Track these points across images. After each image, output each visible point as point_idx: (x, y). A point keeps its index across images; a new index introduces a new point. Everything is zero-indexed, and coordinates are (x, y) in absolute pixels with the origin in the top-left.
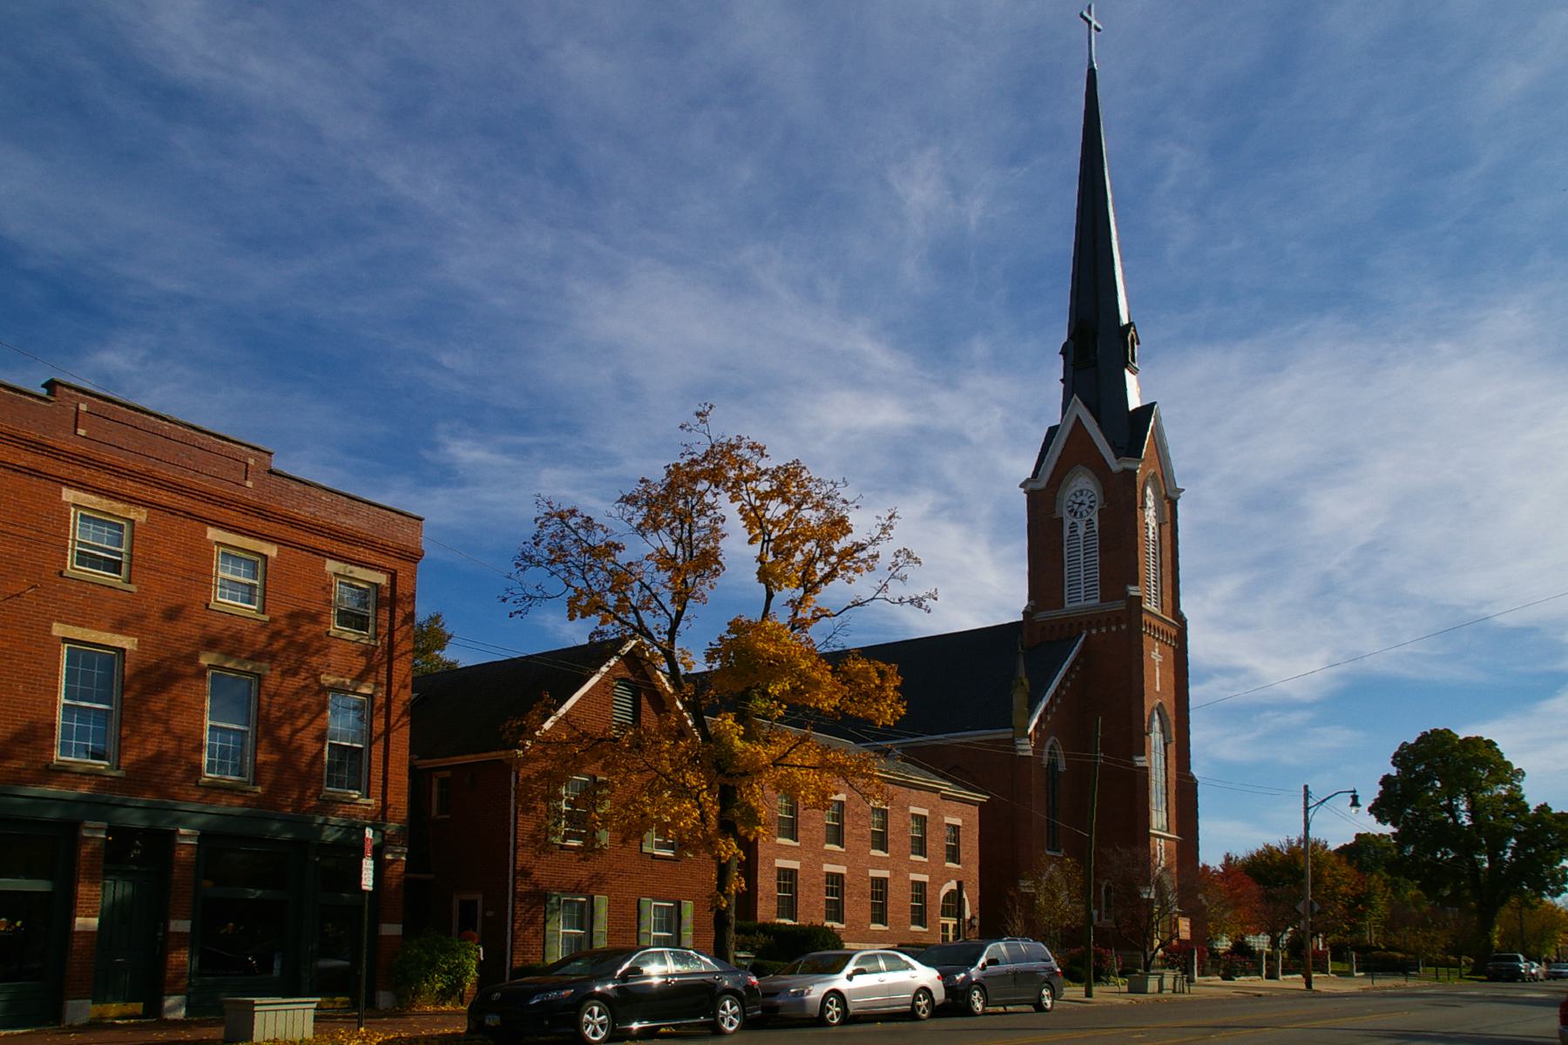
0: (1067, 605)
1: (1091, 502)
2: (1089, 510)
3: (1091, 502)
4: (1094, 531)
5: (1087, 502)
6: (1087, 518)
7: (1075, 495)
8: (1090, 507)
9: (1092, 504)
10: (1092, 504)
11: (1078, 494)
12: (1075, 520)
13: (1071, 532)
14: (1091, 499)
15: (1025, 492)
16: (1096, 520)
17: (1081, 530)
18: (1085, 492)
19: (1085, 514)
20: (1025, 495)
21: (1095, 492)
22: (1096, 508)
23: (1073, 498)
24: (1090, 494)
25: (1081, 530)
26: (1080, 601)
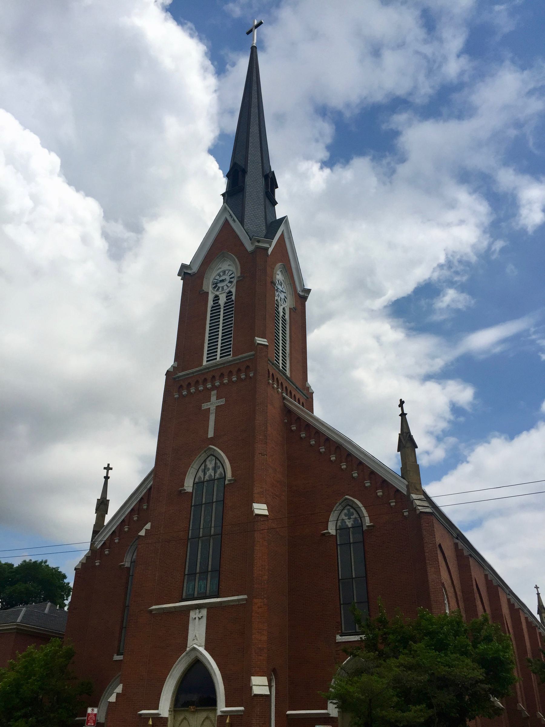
0: (205, 363)
1: (231, 278)
2: (229, 285)
3: (231, 278)
4: (233, 301)
6: (227, 291)
8: (231, 282)
9: (232, 280)
10: (232, 280)
11: (221, 274)
12: (218, 293)
13: (214, 304)
14: (231, 276)
16: (234, 290)
18: (227, 272)
19: (225, 288)
21: (234, 270)
23: (218, 277)
24: (230, 273)
25: (223, 300)
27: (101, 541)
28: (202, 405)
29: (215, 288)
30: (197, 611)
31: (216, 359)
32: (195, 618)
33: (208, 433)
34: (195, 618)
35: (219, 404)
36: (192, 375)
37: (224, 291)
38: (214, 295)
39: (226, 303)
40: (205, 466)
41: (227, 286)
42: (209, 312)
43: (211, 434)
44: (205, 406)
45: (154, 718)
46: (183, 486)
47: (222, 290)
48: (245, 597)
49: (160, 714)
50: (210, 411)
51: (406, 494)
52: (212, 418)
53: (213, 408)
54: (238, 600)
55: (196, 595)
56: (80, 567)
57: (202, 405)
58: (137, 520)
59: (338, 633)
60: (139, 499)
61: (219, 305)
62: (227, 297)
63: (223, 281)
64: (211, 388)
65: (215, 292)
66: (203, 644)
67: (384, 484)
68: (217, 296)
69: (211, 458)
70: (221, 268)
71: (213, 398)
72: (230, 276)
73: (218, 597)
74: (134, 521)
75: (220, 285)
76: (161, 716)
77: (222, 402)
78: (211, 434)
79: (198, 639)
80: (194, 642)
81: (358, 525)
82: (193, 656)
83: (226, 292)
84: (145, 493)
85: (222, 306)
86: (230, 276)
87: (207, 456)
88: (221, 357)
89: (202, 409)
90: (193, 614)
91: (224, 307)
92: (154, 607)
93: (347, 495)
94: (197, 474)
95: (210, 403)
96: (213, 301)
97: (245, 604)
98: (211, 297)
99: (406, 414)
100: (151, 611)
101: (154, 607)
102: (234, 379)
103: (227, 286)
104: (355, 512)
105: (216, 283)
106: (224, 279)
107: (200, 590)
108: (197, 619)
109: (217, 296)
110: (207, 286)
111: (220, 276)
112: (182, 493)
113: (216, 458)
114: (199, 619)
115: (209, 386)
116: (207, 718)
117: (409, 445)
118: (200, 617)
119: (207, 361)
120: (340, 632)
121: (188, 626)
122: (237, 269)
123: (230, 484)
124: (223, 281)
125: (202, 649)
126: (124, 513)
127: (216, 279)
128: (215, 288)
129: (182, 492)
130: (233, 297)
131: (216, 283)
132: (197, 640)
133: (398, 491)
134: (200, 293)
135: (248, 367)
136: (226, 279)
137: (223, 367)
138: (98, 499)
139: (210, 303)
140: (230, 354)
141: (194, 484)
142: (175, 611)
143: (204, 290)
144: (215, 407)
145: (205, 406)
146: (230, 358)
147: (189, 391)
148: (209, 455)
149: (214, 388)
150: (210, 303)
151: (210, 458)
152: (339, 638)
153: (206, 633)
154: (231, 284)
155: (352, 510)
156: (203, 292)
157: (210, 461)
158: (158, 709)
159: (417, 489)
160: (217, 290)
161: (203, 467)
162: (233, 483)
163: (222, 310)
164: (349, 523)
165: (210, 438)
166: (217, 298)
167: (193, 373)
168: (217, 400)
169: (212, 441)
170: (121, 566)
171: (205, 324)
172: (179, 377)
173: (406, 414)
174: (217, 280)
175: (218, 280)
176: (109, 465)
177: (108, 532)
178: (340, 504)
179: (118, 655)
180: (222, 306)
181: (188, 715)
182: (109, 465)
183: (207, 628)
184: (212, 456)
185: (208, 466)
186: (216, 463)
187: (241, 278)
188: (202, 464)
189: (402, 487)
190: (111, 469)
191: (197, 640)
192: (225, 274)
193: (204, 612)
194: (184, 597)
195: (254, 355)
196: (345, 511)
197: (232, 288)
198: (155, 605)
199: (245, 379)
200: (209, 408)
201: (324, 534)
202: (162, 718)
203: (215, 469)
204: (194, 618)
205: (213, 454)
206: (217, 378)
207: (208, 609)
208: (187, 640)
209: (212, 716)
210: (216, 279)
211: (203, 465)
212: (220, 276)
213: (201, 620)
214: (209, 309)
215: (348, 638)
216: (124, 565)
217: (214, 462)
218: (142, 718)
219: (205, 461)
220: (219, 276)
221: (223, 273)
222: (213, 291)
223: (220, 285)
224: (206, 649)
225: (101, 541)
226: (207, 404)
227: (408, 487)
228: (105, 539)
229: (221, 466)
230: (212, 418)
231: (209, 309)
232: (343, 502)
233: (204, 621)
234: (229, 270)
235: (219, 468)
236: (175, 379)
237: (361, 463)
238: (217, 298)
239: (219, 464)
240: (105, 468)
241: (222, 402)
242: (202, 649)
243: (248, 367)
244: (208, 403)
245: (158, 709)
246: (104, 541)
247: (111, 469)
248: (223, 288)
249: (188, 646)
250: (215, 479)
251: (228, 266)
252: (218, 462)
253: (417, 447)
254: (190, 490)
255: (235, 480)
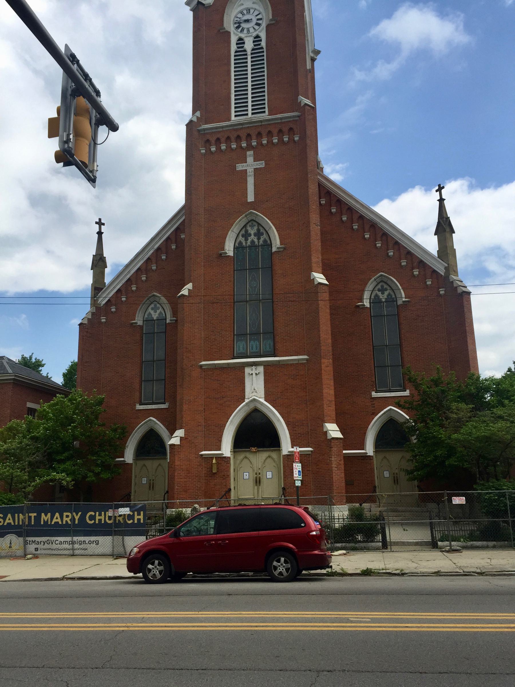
0: (233, 118)
2: (257, 27)
3: (258, 20)
4: (262, 48)
5: (254, 21)
6: (254, 34)
7: (241, 12)
11: (245, 12)
12: (242, 35)
15: (191, 10)
16: (263, 35)
17: (249, 45)
18: (252, 11)
19: (252, 30)
20: (192, 13)
21: (262, 10)
22: (264, 25)
23: (240, 15)
24: (256, 13)
25: (249, 45)
26: (247, 114)
27: (105, 297)
28: (237, 165)
29: (238, 28)
30: (254, 368)
31: (247, 114)
32: (252, 374)
33: (247, 197)
34: (252, 374)
35: (258, 167)
36: (222, 130)
37: (250, 35)
38: (238, 37)
39: (253, 50)
40: (246, 231)
41: (254, 28)
42: (233, 58)
43: (251, 198)
44: (240, 167)
45: (217, 457)
46: (223, 249)
47: (247, 32)
48: (306, 357)
49: (223, 454)
50: (247, 173)
51: (443, 274)
52: (251, 181)
53: (250, 171)
54: (298, 360)
55: (248, 354)
56: (86, 322)
57: (237, 165)
58: (146, 280)
59: (373, 390)
60: (145, 259)
61: (245, 51)
62: (254, 42)
63: (247, 21)
64: (246, 148)
65: (238, 33)
66: (263, 396)
67: (422, 264)
68: (240, 39)
69: (252, 224)
70: (243, 5)
71: (250, 160)
72: (256, 16)
73: (275, 357)
74: (142, 281)
75: (243, 25)
76: (224, 456)
77: (261, 164)
78: (251, 198)
79: (257, 392)
80: (253, 394)
81: (392, 300)
82: (252, 406)
83: (253, 36)
84: (153, 253)
85: (249, 52)
86: (256, 16)
87: (248, 221)
88: (253, 114)
89: (237, 169)
90: (247, 370)
91: (252, 54)
92: (203, 363)
93: (381, 272)
94: (236, 238)
95: (246, 164)
96: (237, 44)
97: (305, 363)
98: (234, 40)
99: (438, 200)
100: (201, 366)
101: (203, 363)
102: (275, 141)
103: (254, 28)
104: (389, 288)
105: (240, 23)
106: (249, 19)
107: (239, 350)
108: (254, 375)
109: (240, 39)
110: (229, 25)
111: (243, 15)
112: (222, 256)
113: (259, 224)
114: (256, 374)
115: (244, 145)
116: (269, 457)
117: (448, 230)
118: (257, 373)
119: (236, 116)
120: (375, 389)
121: (244, 381)
122: (266, 9)
123: (279, 251)
124: (247, 21)
125: (262, 400)
126: (129, 272)
127: (238, 18)
128: (238, 28)
129: (222, 255)
130: (263, 44)
131: (240, 23)
132: (256, 392)
133: (434, 271)
134: (219, 31)
135: (291, 129)
136: (251, 19)
137: (261, 125)
138: (93, 255)
139: (234, 47)
140: (264, 112)
141: (234, 248)
142: (228, 367)
143: (224, 29)
144: (253, 170)
145: (240, 167)
146: (266, 116)
147: (219, 148)
148: (250, 220)
149: (250, 147)
150: (234, 47)
151: (250, 224)
152: (374, 394)
153: (264, 387)
154: (259, 27)
155: (385, 286)
156: (223, 31)
157: (250, 226)
158: (220, 450)
159: (454, 271)
160: (241, 31)
161: (243, 232)
162: (282, 251)
163: (249, 57)
164: (383, 297)
165: (250, 202)
166: (241, 41)
167: (222, 127)
168: (254, 161)
169: (252, 205)
170: (132, 324)
171: (229, 71)
172: (204, 130)
173: (438, 200)
174: (239, 18)
175: (241, 19)
176: (100, 219)
177: (112, 290)
178: (375, 280)
179: (140, 405)
180: (249, 52)
181: (248, 455)
182: (100, 219)
183: (265, 383)
184: (252, 222)
185: (249, 232)
186: (258, 230)
187: (274, 22)
188: (241, 229)
189: (440, 268)
190: (104, 224)
191: (256, 392)
192: (249, 12)
193: (261, 369)
194: (235, 355)
195: (299, 116)
196: (379, 286)
197: (260, 32)
198: (204, 361)
199: (288, 142)
200: (246, 170)
201: (358, 306)
202: (225, 457)
203: (258, 234)
204: (251, 374)
205: (254, 219)
206: (254, 137)
207: (264, 366)
208: (245, 392)
209: (274, 455)
210: (238, 18)
211: (244, 229)
212: (243, 15)
213: (258, 376)
214: (233, 54)
215: (400, 394)
216: (136, 323)
217: (256, 228)
218: (203, 458)
219: (245, 226)
220: (242, 13)
221: (247, 11)
222: (235, 32)
223: (243, 25)
224: (266, 400)
225: (105, 297)
226: (243, 164)
227: (446, 268)
228: (110, 295)
229: (264, 232)
230: (251, 181)
231: (233, 54)
232: (378, 277)
233: (262, 377)
234: (255, 9)
235: (262, 234)
236: (199, 131)
237: (397, 243)
238: (241, 41)
239: (262, 230)
240: (96, 223)
241: (261, 164)
242: (262, 400)
243: (291, 129)
244: (244, 164)
245: (219, 449)
246: (109, 298)
247: (104, 224)
248: (248, 30)
249: (246, 398)
250: (259, 245)
251: (253, 3)
252: (261, 228)
253: (454, 233)
254: (231, 254)
255: (285, 248)
